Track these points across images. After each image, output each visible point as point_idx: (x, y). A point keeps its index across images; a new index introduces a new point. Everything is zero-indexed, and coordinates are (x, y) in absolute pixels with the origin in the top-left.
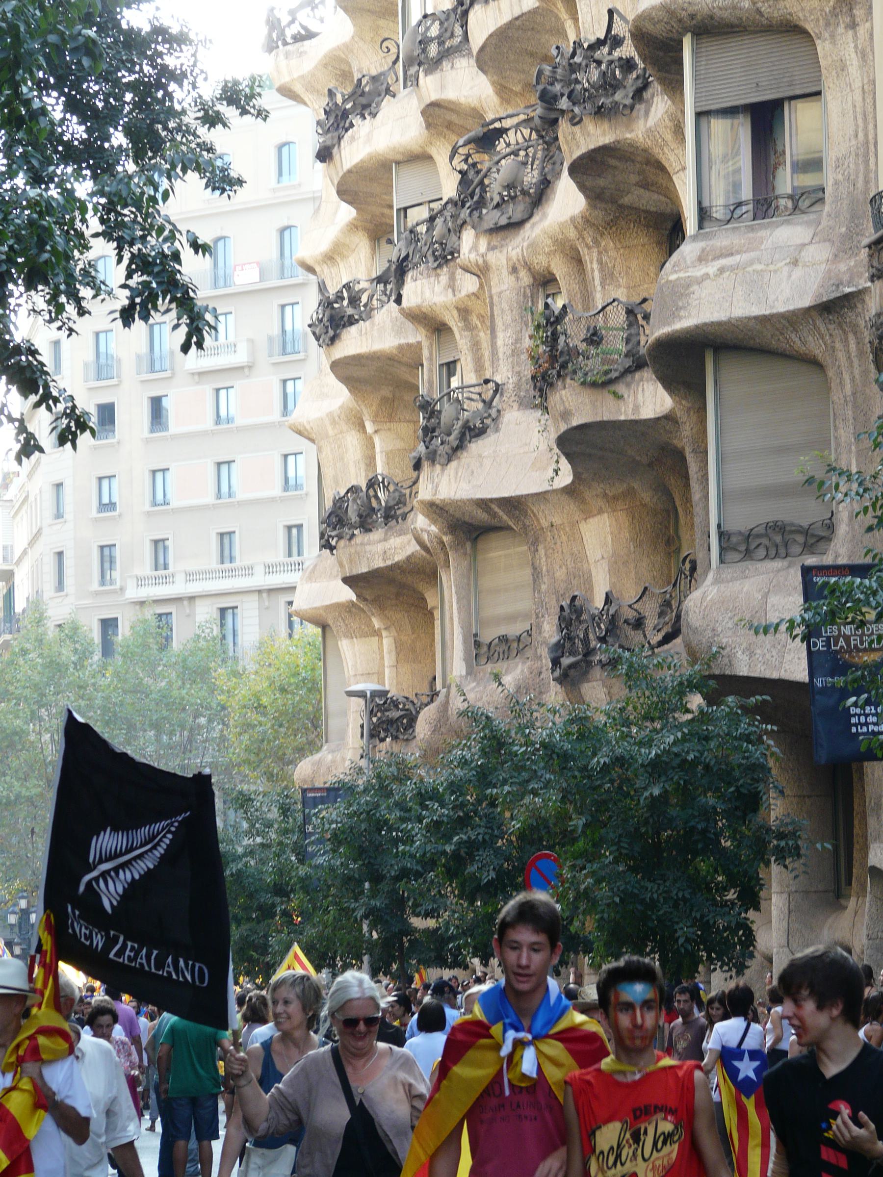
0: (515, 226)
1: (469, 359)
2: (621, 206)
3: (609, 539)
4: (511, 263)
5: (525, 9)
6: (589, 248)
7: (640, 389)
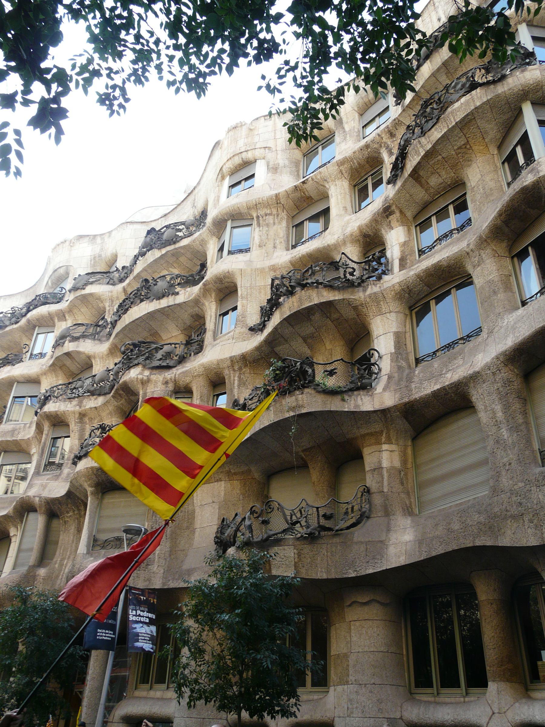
0: (168, 367)
1: (77, 434)
2: (274, 350)
3: (223, 493)
4: (165, 380)
5: (177, 302)
6: (234, 370)
7: (359, 398)
